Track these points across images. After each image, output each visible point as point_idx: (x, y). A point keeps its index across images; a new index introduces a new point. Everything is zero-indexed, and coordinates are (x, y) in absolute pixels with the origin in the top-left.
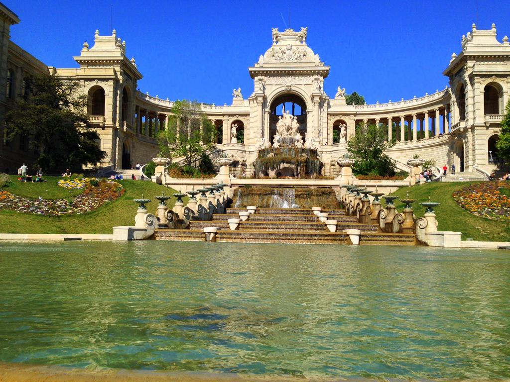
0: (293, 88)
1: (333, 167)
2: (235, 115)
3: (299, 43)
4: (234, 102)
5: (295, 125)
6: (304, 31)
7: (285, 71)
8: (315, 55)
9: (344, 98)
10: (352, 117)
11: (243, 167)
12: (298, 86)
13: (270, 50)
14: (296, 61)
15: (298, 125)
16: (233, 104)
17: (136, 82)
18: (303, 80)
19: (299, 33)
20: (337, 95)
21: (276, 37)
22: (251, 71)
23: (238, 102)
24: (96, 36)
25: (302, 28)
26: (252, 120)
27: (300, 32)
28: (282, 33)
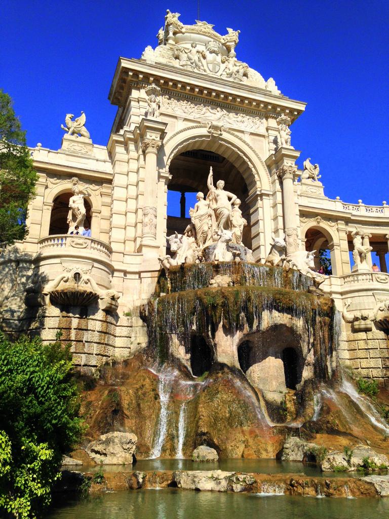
0: (226, 136)
1: (362, 335)
2: (69, 176)
6: (233, 35)
7: (210, 91)
8: (266, 80)
9: (320, 184)
10: (341, 225)
11: (110, 319)
12: (236, 133)
16: (63, 147)
18: (245, 124)
19: (223, 39)
21: (175, 33)
23: (77, 147)
25: (230, 30)
26: (119, 193)
27: (224, 37)
28: (189, 26)
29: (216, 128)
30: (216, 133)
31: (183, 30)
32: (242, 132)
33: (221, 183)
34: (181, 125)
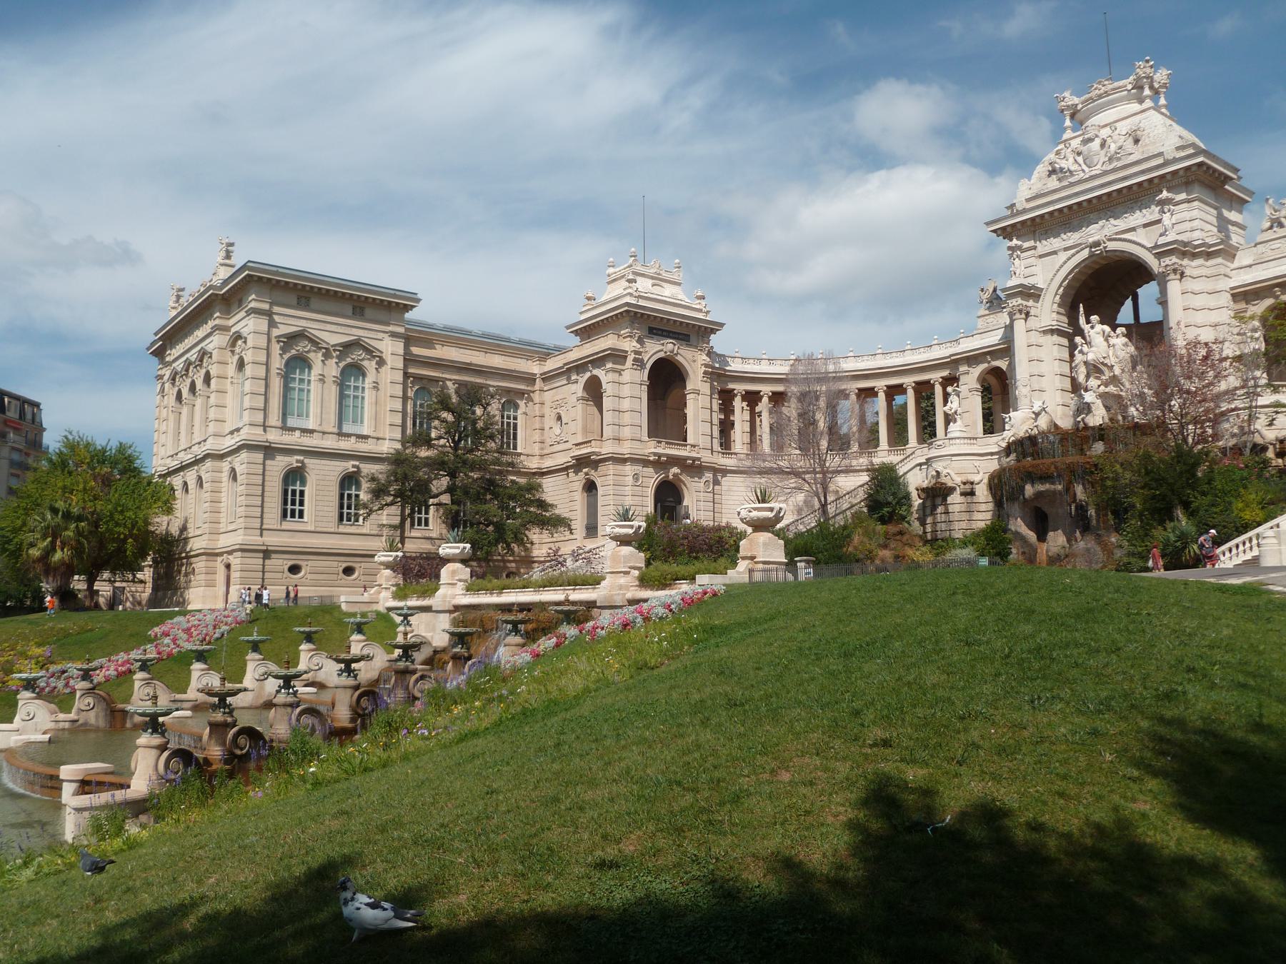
0: (1112, 246)
3: (1135, 107)
14: (1111, 167)
29: (1097, 244)
30: (1097, 251)
31: (1079, 107)
32: (1133, 229)
33: (1095, 318)
34: (1063, 256)
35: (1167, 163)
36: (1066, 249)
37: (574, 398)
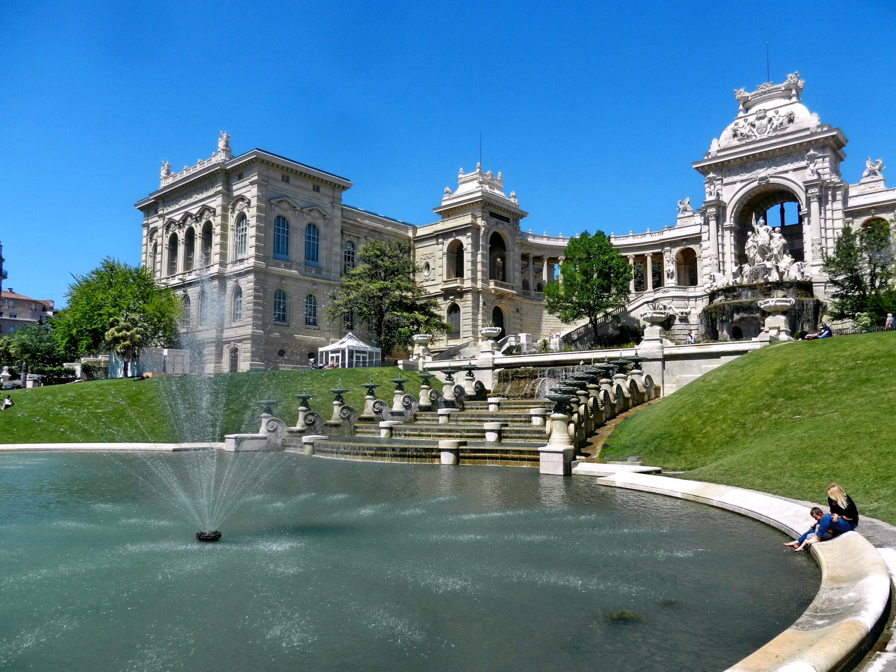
0: (772, 180)
3: (787, 101)
4: (678, 221)
5: (778, 241)
13: (732, 126)
14: (775, 134)
15: (783, 241)
17: (517, 224)
20: (866, 173)
22: (697, 168)
24: (460, 176)
32: (787, 172)
34: (739, 186)
35: (812, 135)
36: (742, 181)
37: (441, 253)
